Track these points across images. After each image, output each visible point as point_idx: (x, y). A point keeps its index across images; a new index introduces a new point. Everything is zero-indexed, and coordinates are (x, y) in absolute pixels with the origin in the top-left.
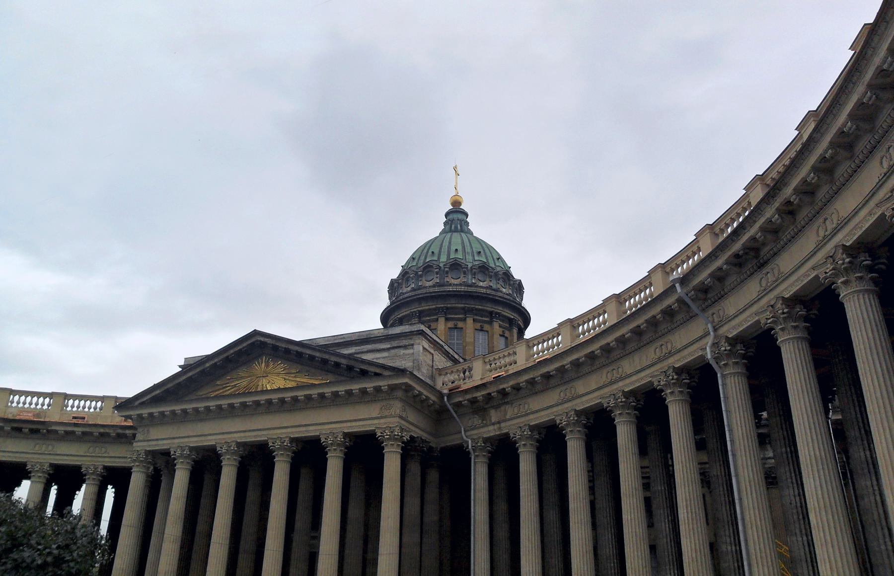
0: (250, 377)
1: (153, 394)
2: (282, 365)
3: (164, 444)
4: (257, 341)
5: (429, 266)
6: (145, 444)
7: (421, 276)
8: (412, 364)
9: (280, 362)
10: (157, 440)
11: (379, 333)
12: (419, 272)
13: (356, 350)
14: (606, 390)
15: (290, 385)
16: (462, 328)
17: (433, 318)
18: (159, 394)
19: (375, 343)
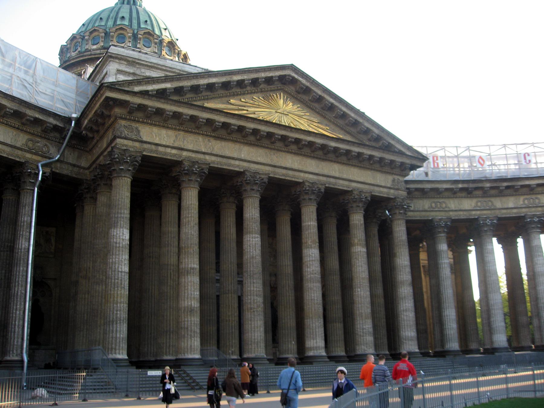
0: (268, 108)
3: (166, 154)
4: (289, 75)
5: (149, 33)
6: (137, 144)
7: (140, 39)
10: (157, 145)
18: (169, 89)
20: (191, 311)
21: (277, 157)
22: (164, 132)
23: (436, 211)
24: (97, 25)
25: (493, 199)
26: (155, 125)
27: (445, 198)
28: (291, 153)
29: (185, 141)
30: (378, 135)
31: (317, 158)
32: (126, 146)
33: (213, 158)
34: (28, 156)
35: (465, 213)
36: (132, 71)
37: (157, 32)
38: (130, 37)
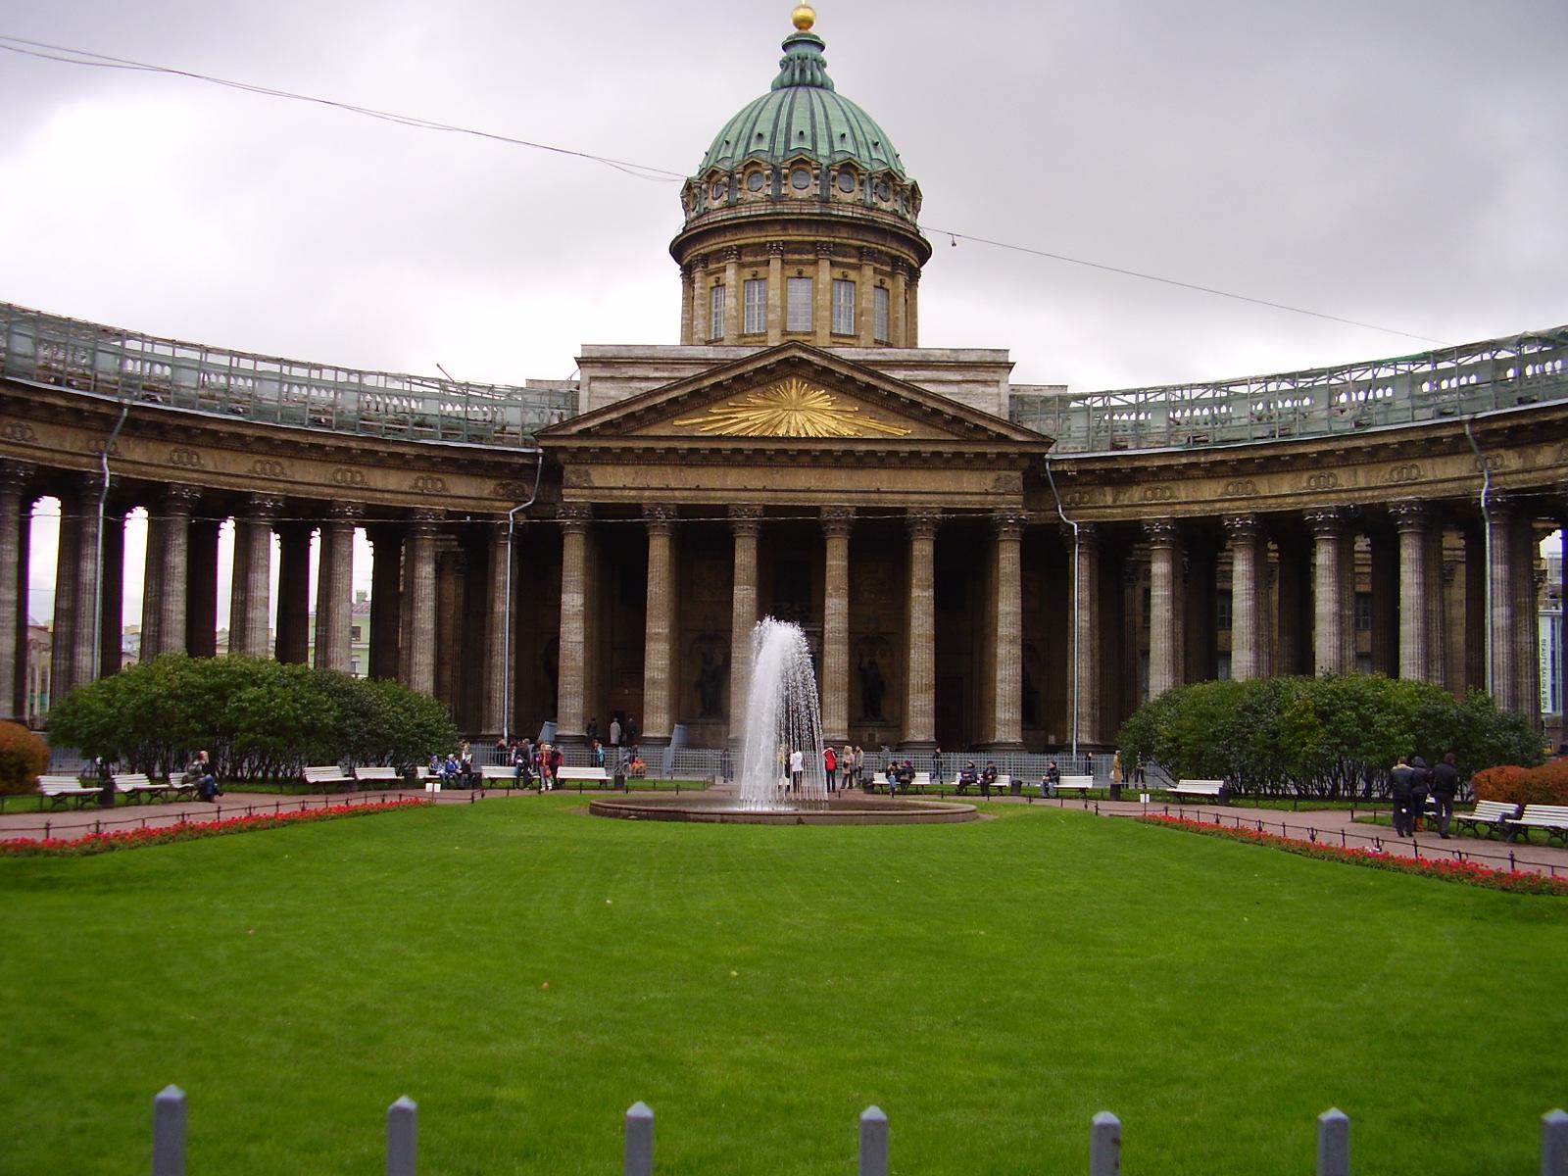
0: (771, 407)
1: (607, 418)
2: (828, 396)
3: (623, 497)
4: (794, 357)
5: (801, 161)
6: (586, 492)
7: (786, 177)
8: (996, 409)
9: (823, 391)
11: (942, 355)
12: (784, 168)
13: (906, 376)
14: (1305, 498)
15: (847, 431)
16: (854, 282)
17: (806, 257)
18: (616, 419)
19: (938, 370)
20: (654, 682)
21: (782, 476)
22: (621, 469)
23: (1151, 505)
24: (720, 157)
25: (1254, 479)
26: (608, 464)
27: (1168, 480)
28: (803, 466)
29: (648, 477)
30: (954, 417)
31: (847, 467)
32: (574, 496)
33: (686, 494)
34: (498, 504)
35: (1202, 506)
36: (609, 375)
37: (823, 149)
38: (768, 178)
